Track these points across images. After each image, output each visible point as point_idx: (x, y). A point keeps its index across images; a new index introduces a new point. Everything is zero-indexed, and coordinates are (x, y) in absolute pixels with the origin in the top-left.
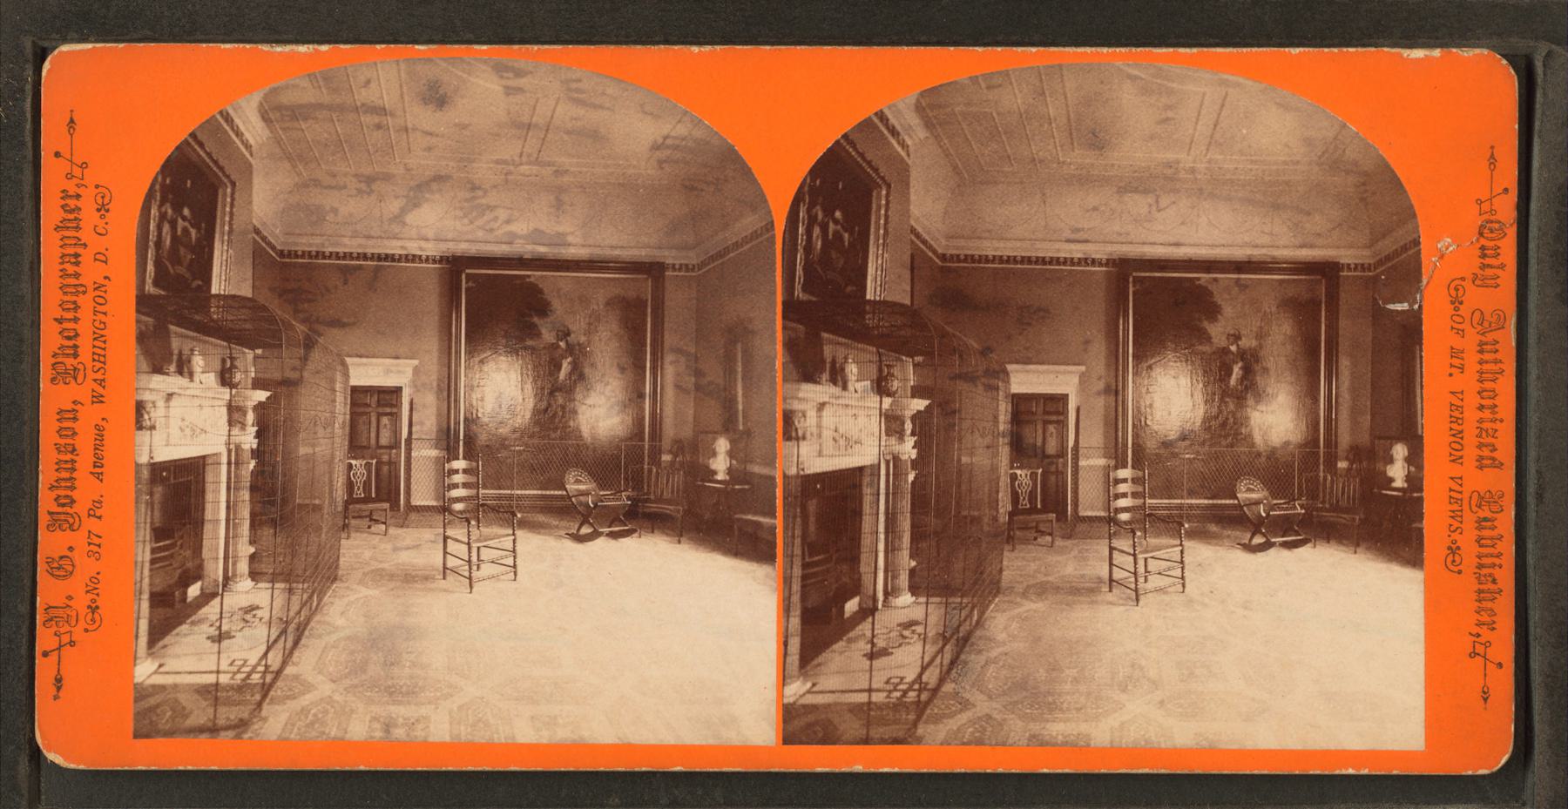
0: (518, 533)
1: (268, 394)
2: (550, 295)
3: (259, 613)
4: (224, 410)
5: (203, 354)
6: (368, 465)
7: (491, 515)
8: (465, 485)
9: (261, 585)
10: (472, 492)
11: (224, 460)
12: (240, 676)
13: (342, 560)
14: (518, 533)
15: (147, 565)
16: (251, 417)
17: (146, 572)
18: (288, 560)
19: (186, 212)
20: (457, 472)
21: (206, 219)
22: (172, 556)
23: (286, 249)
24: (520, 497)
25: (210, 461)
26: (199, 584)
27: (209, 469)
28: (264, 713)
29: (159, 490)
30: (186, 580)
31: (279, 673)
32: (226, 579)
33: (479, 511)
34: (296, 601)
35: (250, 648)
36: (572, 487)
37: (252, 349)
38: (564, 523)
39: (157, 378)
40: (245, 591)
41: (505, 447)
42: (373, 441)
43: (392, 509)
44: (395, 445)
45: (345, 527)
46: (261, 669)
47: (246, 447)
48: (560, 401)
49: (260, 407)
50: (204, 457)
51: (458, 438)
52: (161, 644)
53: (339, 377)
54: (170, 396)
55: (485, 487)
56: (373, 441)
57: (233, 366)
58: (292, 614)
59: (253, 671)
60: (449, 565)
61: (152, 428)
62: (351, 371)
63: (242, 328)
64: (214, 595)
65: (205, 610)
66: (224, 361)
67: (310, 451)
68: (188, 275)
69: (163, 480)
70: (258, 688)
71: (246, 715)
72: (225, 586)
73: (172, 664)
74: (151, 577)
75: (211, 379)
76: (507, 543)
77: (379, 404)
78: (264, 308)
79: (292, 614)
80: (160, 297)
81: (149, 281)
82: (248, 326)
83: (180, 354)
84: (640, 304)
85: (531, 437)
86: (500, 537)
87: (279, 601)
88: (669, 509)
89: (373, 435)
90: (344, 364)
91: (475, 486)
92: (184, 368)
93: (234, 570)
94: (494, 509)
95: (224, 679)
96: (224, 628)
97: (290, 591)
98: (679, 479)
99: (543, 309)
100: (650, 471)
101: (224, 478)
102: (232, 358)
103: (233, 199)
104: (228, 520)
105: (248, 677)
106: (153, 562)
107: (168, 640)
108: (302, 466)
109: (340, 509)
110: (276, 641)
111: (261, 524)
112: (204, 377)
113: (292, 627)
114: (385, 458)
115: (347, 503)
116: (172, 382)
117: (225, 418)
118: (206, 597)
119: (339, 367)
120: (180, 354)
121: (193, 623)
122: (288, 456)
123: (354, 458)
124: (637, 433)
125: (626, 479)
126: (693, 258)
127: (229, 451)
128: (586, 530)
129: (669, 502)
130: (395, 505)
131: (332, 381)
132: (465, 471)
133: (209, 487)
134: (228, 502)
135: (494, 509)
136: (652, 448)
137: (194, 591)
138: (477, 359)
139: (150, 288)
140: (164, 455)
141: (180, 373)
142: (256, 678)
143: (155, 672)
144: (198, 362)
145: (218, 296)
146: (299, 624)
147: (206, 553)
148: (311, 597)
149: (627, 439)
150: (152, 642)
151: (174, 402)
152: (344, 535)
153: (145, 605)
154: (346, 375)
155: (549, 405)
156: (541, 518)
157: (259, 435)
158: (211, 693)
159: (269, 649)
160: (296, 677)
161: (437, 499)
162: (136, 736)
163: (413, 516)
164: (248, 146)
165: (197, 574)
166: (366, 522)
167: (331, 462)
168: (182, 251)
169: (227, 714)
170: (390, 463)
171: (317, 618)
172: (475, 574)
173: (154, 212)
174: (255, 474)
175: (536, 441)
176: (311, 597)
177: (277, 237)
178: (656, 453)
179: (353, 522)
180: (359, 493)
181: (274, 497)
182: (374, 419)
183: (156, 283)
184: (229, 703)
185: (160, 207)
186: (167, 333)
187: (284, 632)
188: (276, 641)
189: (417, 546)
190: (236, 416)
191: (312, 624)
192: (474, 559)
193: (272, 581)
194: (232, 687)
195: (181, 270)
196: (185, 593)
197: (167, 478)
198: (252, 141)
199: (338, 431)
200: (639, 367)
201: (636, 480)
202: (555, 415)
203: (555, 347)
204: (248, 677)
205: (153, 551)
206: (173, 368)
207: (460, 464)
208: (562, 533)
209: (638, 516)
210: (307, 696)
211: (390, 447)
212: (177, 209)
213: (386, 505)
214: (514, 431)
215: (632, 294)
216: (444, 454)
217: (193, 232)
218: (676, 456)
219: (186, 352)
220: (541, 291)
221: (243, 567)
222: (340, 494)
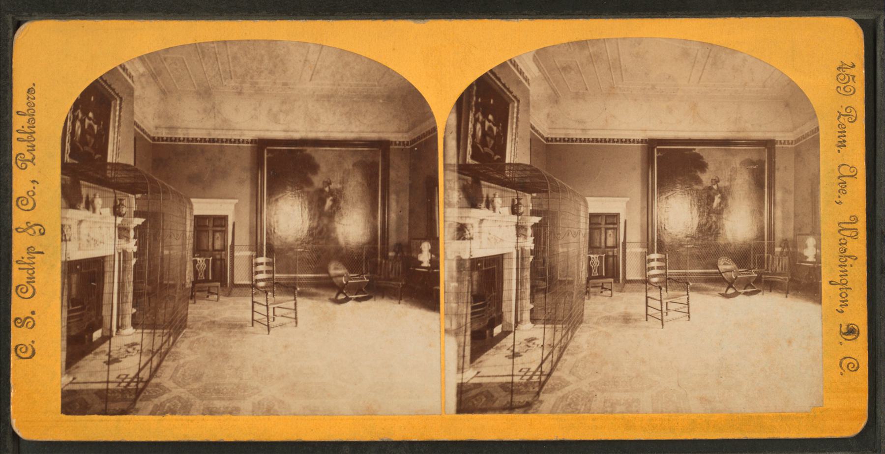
0: (691, 294)
1: (540, 218)
2: (706, 159)
3: (537, 342)
4: (514, 228)
5: (501, 197)
6: (600, 258)
7: (674, 284)
8: (658, 268)
9: (537, 326)
10: (663, 272)
11: (515, 256)
12: (526, 378)
13: (585, 312)
14: (691, 294)
15: (469, 317)
16: (530, 232)
17: (469, 320)
18: (553, 311)
19: (490, 117)
20: (653, 260)
21: (502, 120)
22: (484, 311)
23: (549, 136)
24: (691, 274)
25: (505, 257)
26: (500, 326)
27: (506, 262)
28: (541, 398)
29: (476, 275)
30: (492, 325)
31: (549, 375)
32: (517, 323)
33: (667, 282)
34: (558, 336)
35: (531, 360)
36: (722, 268)
37: (530, 192)
38: (718, 288)
39: (474, 211)
40: (527, 330)
41: (681, 246)
42: (603, 244)
43: (615, 282)
44: (616, 246)
45: (587, 292)
46: (538, 373)
47: (528, 249)
48: (714, 219)
49: (535, 226)
50: (502, 255)
51: (655, 242)
52: (478, 360)
53: (582, 208)
54: (482, 220)
55: (670, 268)
56: (603, 244)
57: (519, 203)
58: (556, 342)
59: (534, 374)
60: (649, 313)
61: (471, 239)
62: (589, 203)
63: (527, 182)
64: (509, 332)
65: (504, 341)
66: (513, 201)
67: (565, 250)
68: (491, 152)
69: (478, 269)
70: (537, 384)
71: (530, 399)
72: (516, 327)
73: (484, 371)
74: (472, 323)
75: (506, 210)
76: (684, 299)
77: (606, 224)
78: (537, 170)
79: (556, 342)
80: (476, 165)
81: (469, 157)
82: (528, 180)
83: (488, 197)
84: (761, 163)
85: (697, 240)
86: (680, 296)
87: (549, 335)
88: (780, 278)
89: (603, 241)
90: (585, 202)
91: (665, 268)
92: (490, 204)
93: (521, 318)
94: (676, 281)
95: (516, 379)
96: (516, 350)
97: (555, 330)
98: (785, 260)
99: (703, 167)
100: (768, 257)
101: (514, 266)
102: (518, 199)
103: (518, 110)
104: (517, 290)
105: (531, 378)
106: (472, 314)
107: (484, 357)
108: (560, 258)
109: (584, 282)
110: (546, 358)
111: (538, 291)
112: (501, 210)
113: (557, 349)
114: (611, 253)
115: (588, 279)
116: (481, 213)
117: (515, 232)
118: (505, 334)
119: (582, 203)
120: (488, 197)
121: (498, 348)
122: (553, 254)
123: (592, 253)
124: (761, 237)
125: (754, 263)
126: (790, 137)
127: (518, 251)
128: (731, 291)
129: (780, 274)
130: (617, 280)
131: (578, 211)
132: (658, 260)
133: (506, 272)
134: (517, 280)
135: (676, 281)
136: (769, 245)
137: (497, 330)
138: (664, 197)
139: (469, 160)
140: (479, 253)
141: (488, 207)
142: (535, 378)
143: (475, 376)
144: (498, 201)
145: (510, 164)
146: (561, 348)
147: (505, 308)
148: (567, 332)
149: (754, 240)
150: (472, 360)
151: (484, 224)
152: (586, 297)
153: (468, 338)
154: (587, 207)
155: (708, 222)
156: (704, 285)
157: (535, 241)
158: (509, 388)
159: (543, 362)
160: (559, 378)
161: (642, 276)
162: (460, 411)
163: (628, 285)
164: (527, 80)
165: (499, 319)
166: (599, 289)
167: (579, 255)
168: (488, 139)
169: (519, 399)
170: (613, 256)
171: (572, 344)
172: (665, 318)
173: (471, 117)
174: (533, 265)
175: (700, 242)
176: (567, 332)
177: (545, 130)
178: (771, 247)
179: (592, 290)
180: (595, 273)
181: (544, 277)
182: (603, 232)
183: (472, 157)
184: (519, 393)
185: (475, 115)
186: (480, 185)
187: (551, 352)
188: (546, 358)
189: (631, 301)
190: (522, 231)
191: (568, 347)
192: (664, 309)
193: (544, 324)
194: (521, 384)
195: (487, 150)
196: (492, 331)
197: (481, 267)
198: (529, 77)
199: (582, 239)
200: (761, 198)
201: (761, 263)
202: (711, 226)
203: (710, 188)
204: (531, 378)
205: (473, 308)
206: (483, 205)
207: (655, 256)
208: (717, 293)
209: (764, 283)
210: (567, 388)
211: (613, 247)
212: (485, 116)
213: (612, 280)
214: (687, 237)
215: (755, 157)
216: (646, 250)
217: (495, 128)
218: (784, 248)
219: (491, 196)
220: (701, 157)
221: (527, 315)
222: (584, 275)
